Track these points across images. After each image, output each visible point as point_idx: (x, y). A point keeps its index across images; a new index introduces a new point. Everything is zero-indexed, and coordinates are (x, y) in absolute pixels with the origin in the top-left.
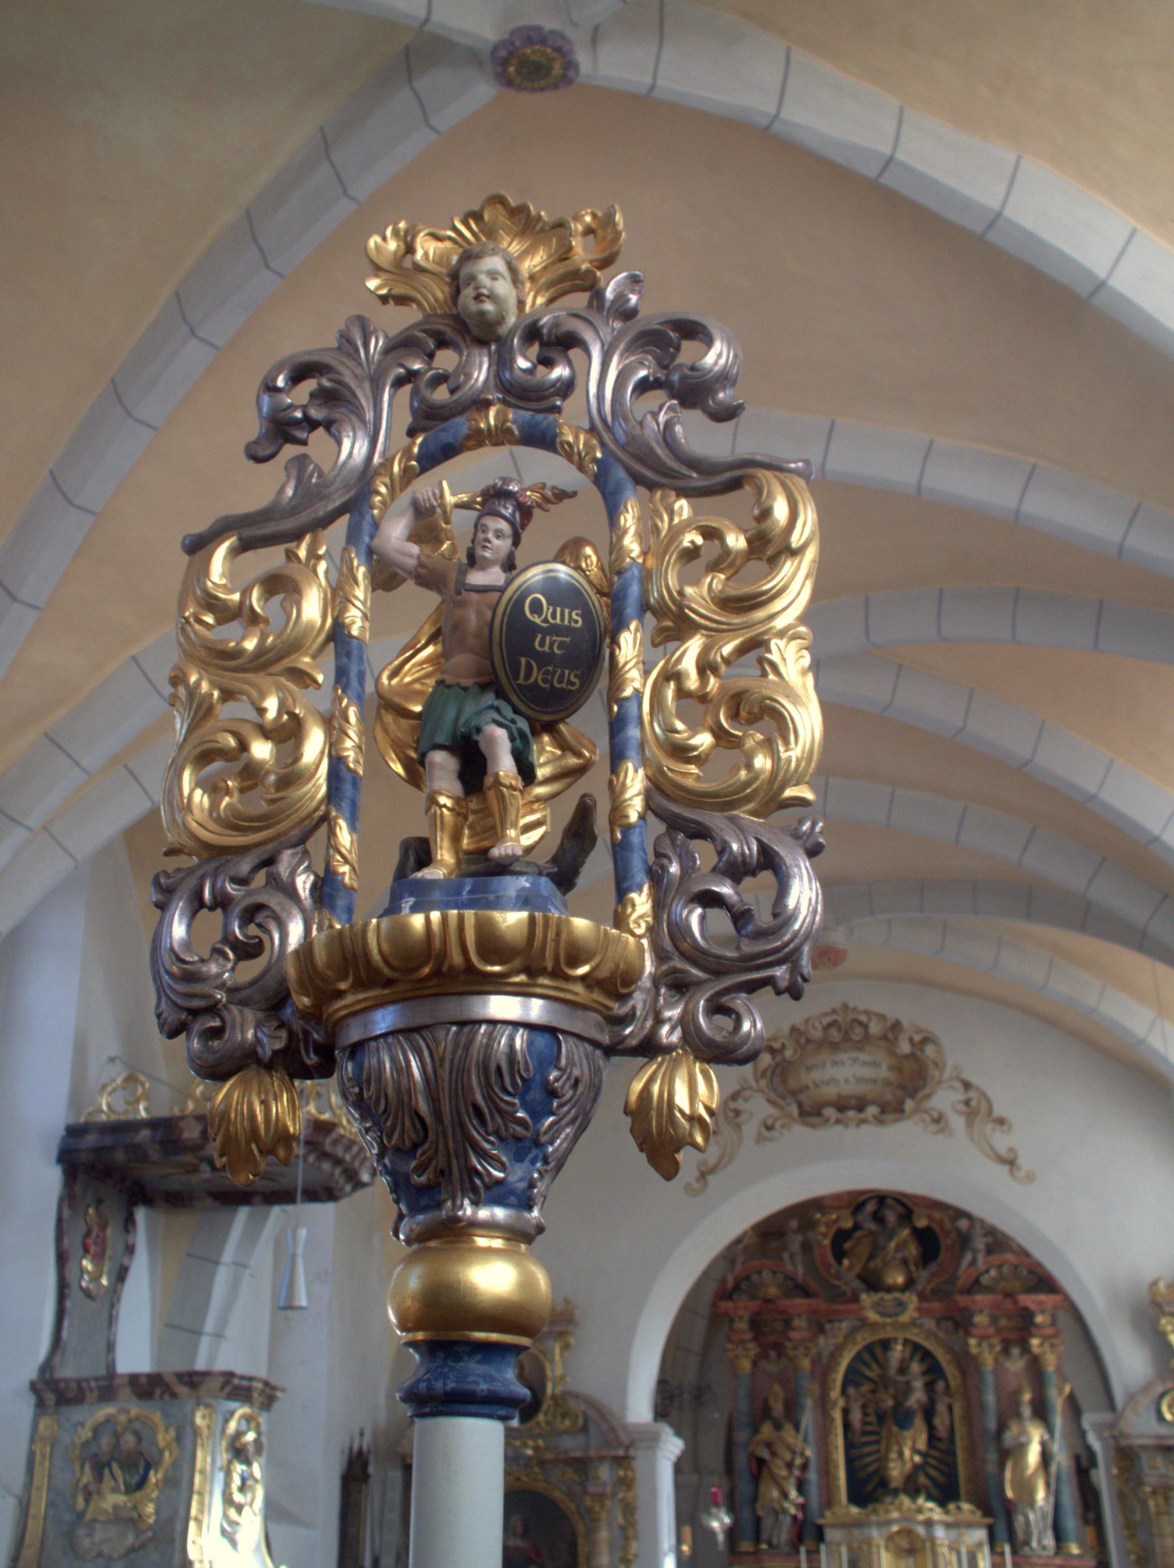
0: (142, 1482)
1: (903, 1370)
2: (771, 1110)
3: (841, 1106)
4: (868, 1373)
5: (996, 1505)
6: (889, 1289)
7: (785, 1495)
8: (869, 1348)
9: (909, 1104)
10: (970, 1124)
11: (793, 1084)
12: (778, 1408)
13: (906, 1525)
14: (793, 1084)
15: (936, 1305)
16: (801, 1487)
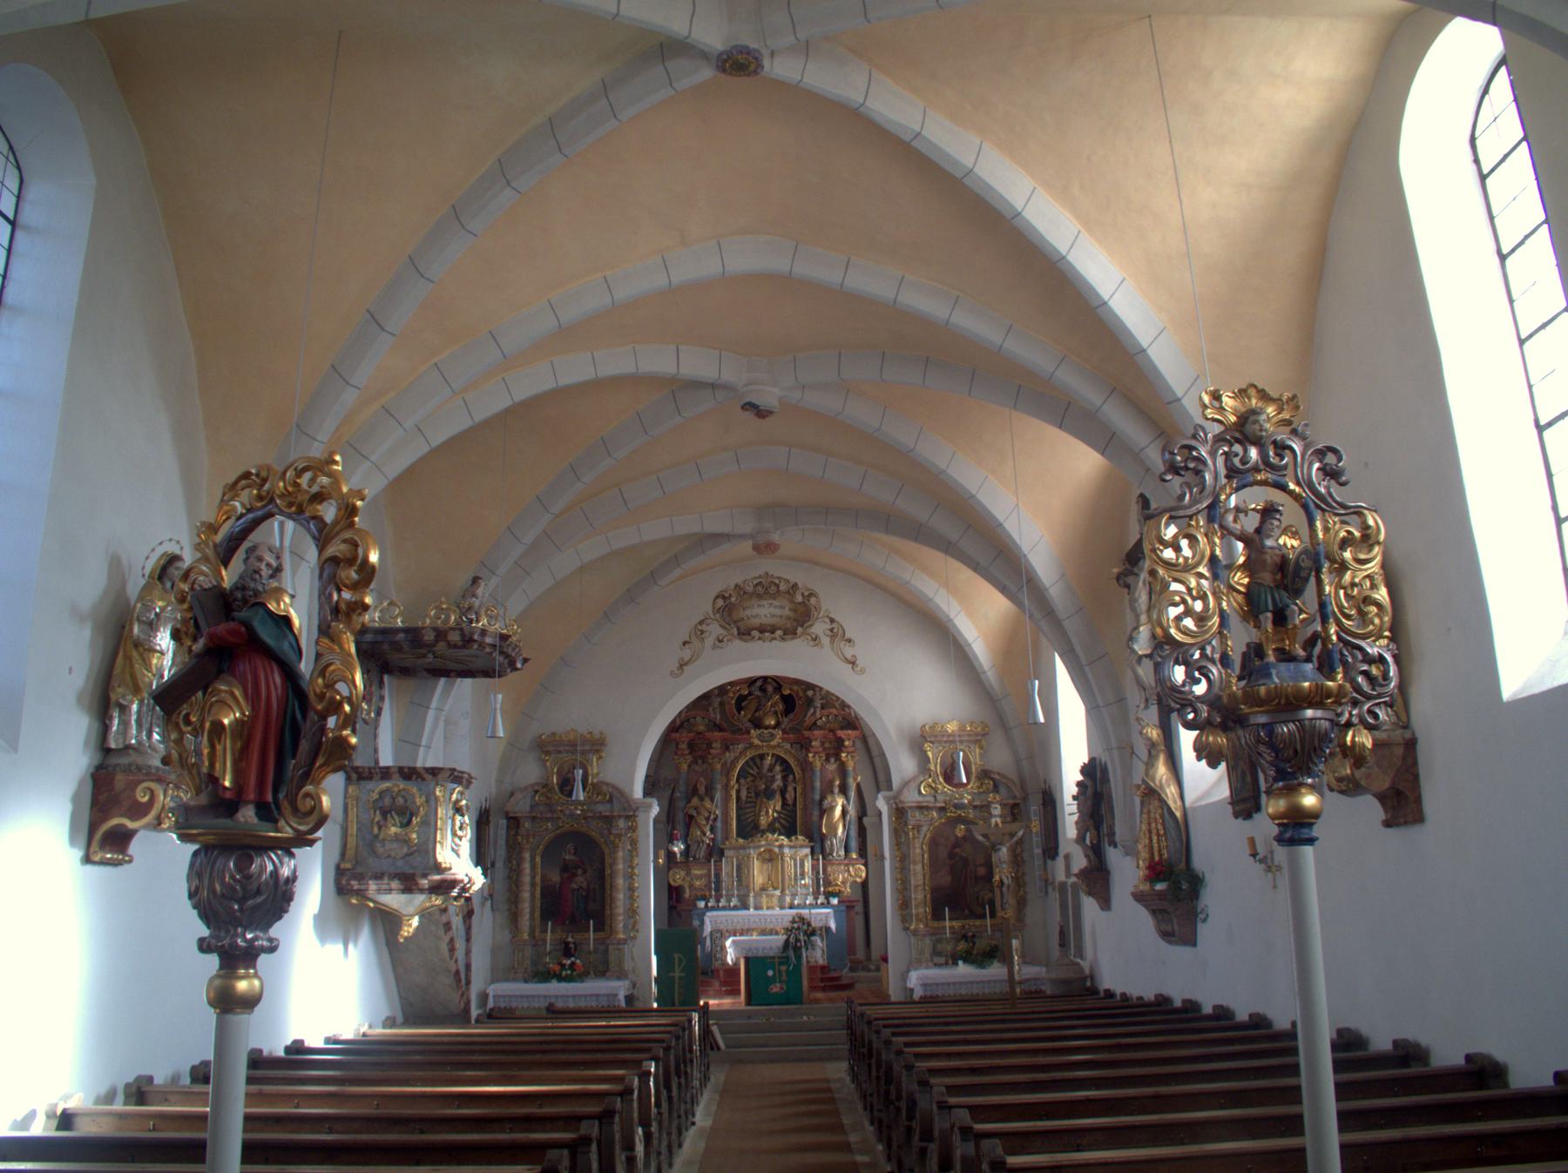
0: (409, 822)
1: (771, 769)
2: (722, 631)
3: (762, 630)
5: (816, 835)
6: (767, 728)
8: (752, 759)
9: (800, 630)
10: (832, 642)
11: (735, 617)
14: (735, 617)
16: (712, 830)
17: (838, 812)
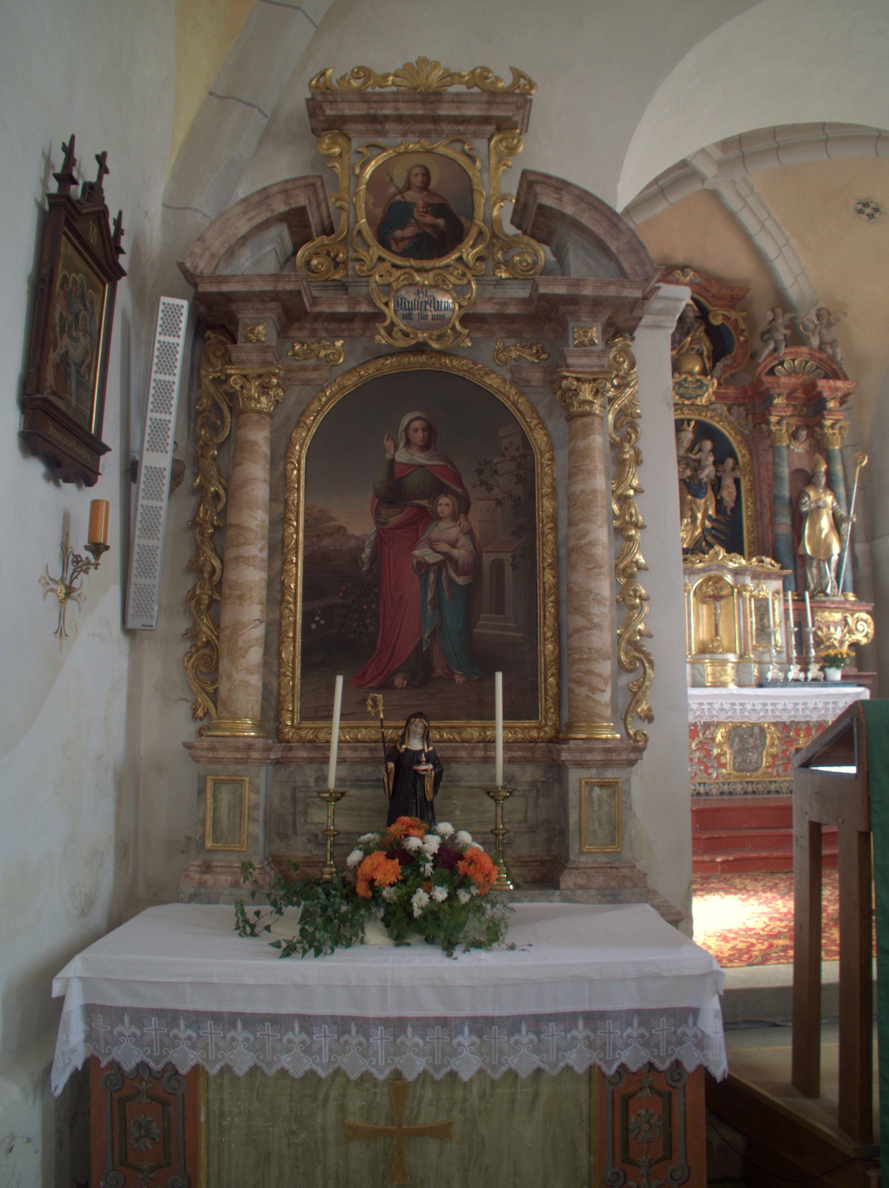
17: (825, 523)
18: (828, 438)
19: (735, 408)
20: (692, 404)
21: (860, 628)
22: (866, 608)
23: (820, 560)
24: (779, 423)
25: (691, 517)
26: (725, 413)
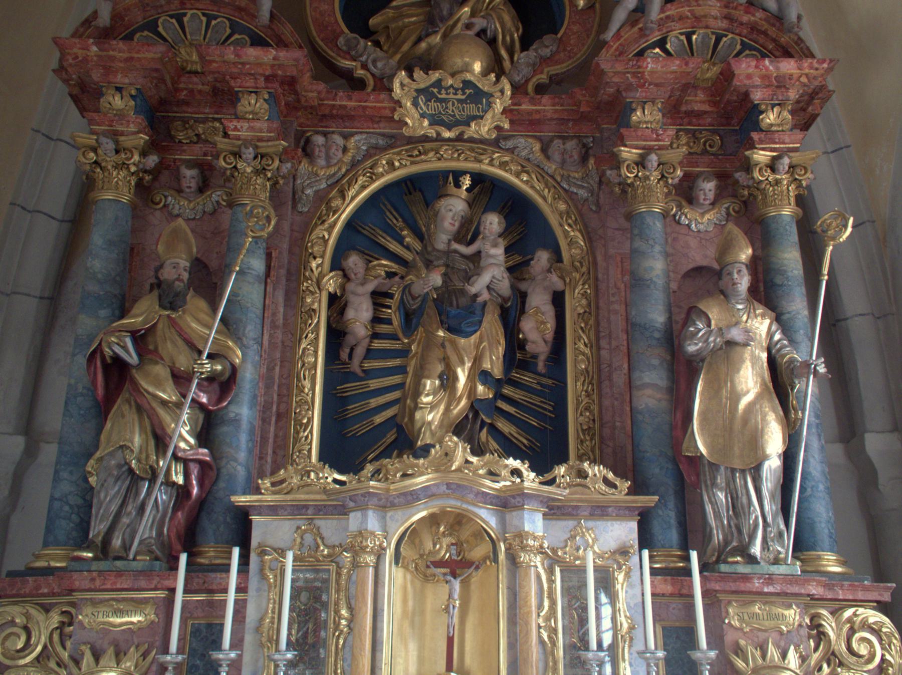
1: (468, 232)
4: (394, 247)
5: (658, 470)
7: (161, 440)
12: (177, 267)
13: (452, 504)
15: (546, 106)
17: (749, 379)
18: (763, 192)
19: (557, 142)
20: (459, 138)
21: (863, 650)
22: (875, 596)
23: (733, 471)
24: (641, 163)
25: (440, 377)
26: (538, 155)
